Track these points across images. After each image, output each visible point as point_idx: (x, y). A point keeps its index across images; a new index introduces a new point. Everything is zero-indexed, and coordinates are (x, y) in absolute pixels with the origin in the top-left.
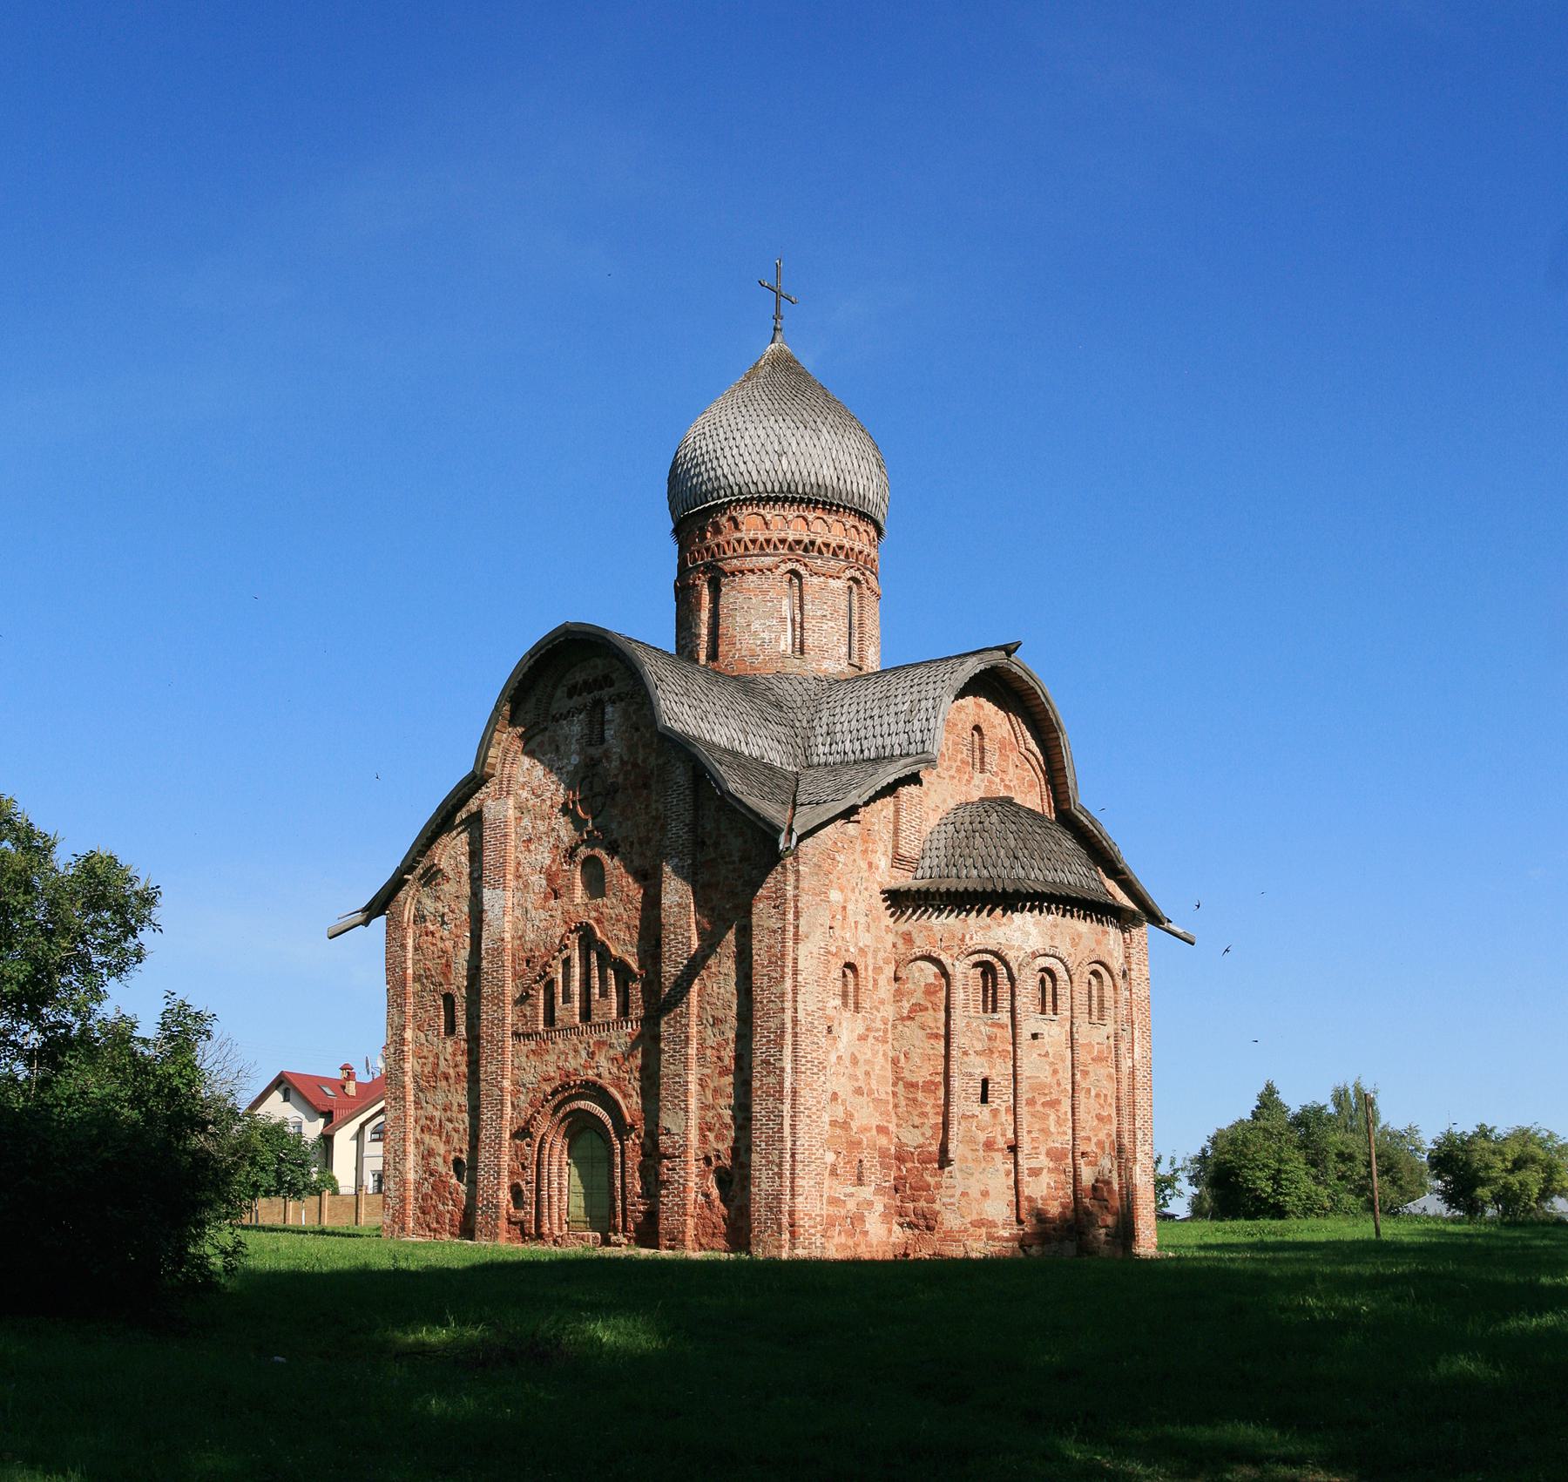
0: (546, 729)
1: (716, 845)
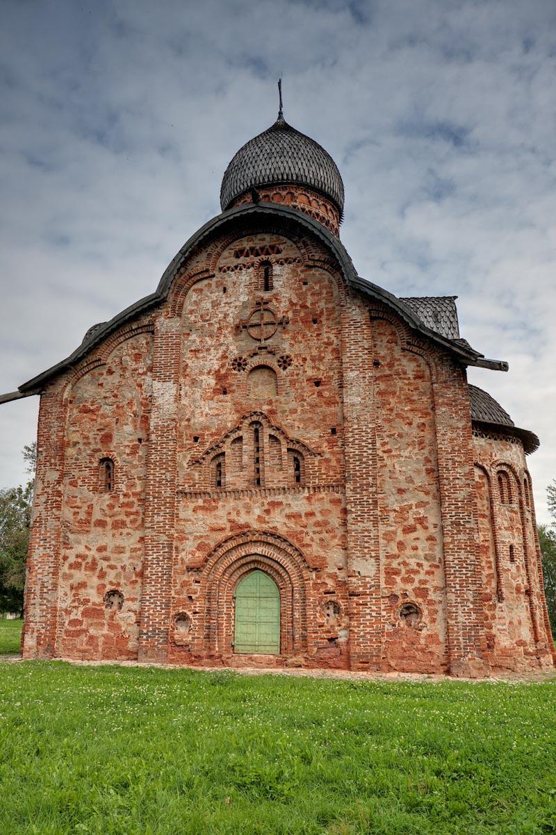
0: (214, 276)
1: (390, 365)
